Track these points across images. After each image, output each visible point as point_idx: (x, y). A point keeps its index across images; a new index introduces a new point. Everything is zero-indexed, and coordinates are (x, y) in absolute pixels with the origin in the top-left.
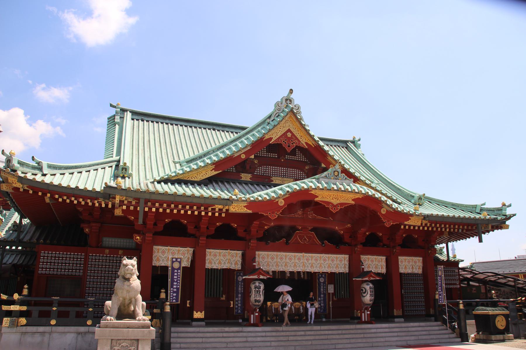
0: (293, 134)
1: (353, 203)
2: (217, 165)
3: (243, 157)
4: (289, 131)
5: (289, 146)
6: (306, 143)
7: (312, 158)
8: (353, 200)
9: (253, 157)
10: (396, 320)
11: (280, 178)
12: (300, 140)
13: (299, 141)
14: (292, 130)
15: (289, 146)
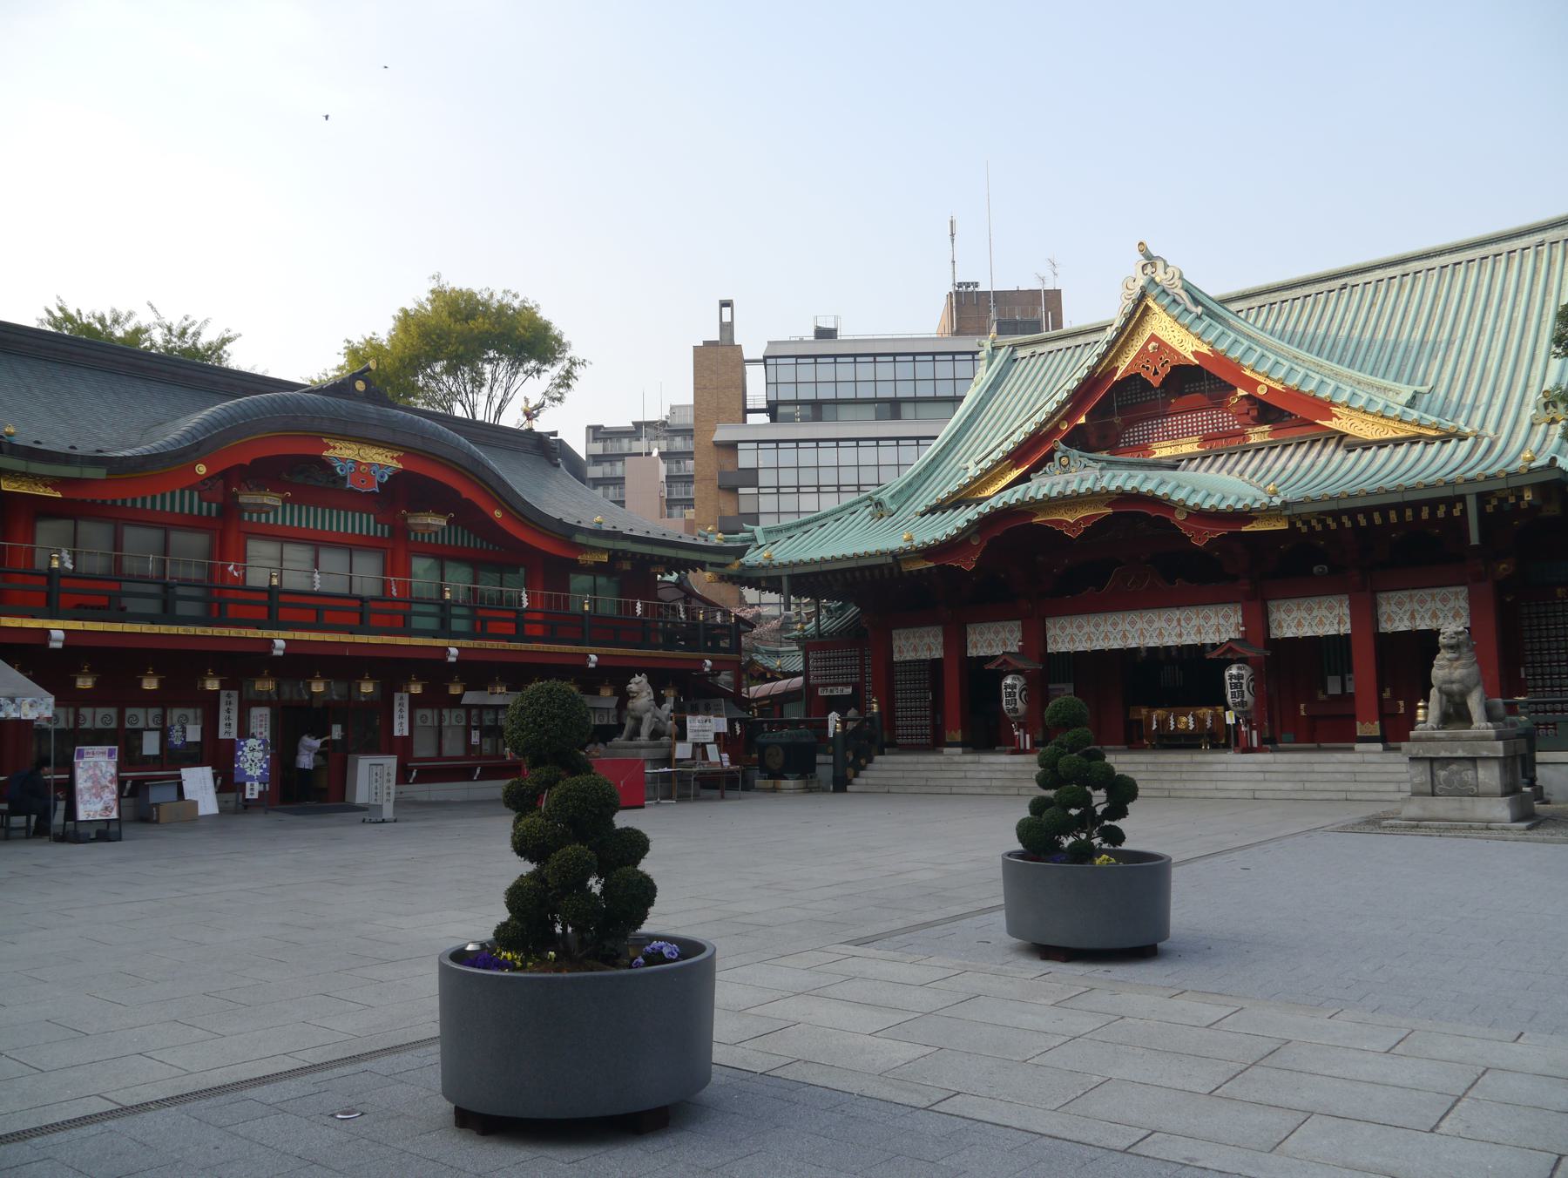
0: (1162, 346)
1: (1110, 511)
2: (1016, 456)
3: (1065, 427)
4: (1153, 338)
5: (1156, 373)
6: (1196, 354)
7: (1196, 385)
8: (1108, 506)
9: (1082, 420)
10: (1358, 746)
11: (1168, 443)
12: (1180, 350)
13: (1178, 354)
14: (1160, 334)
15: (1156, 373)
